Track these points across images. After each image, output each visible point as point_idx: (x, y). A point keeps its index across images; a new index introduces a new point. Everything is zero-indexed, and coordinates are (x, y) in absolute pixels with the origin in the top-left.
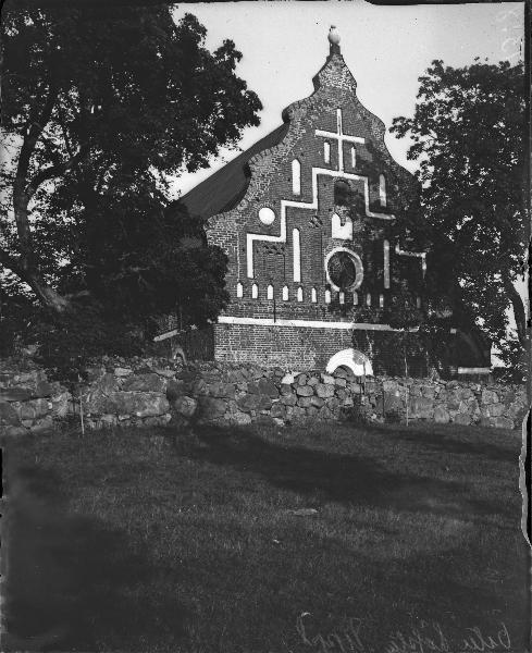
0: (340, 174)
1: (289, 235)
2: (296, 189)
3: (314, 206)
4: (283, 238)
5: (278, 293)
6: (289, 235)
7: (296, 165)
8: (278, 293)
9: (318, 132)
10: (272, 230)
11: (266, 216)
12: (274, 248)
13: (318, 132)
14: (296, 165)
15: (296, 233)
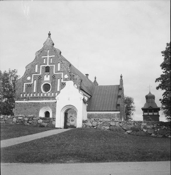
0: (48, 65)
1: (34, 82)
2: (36, 71)
3: (40, 74)
4: (32, 83)
5: (30, 95)
6: (34, 82)
7: (37, 66)
8: (30, 95)
9: (42, 57)
10: (30, 81)
11: (29, 78)
12: (29, 85)
13: (42, 57)
14: (37, 66)
15: (35, 81)
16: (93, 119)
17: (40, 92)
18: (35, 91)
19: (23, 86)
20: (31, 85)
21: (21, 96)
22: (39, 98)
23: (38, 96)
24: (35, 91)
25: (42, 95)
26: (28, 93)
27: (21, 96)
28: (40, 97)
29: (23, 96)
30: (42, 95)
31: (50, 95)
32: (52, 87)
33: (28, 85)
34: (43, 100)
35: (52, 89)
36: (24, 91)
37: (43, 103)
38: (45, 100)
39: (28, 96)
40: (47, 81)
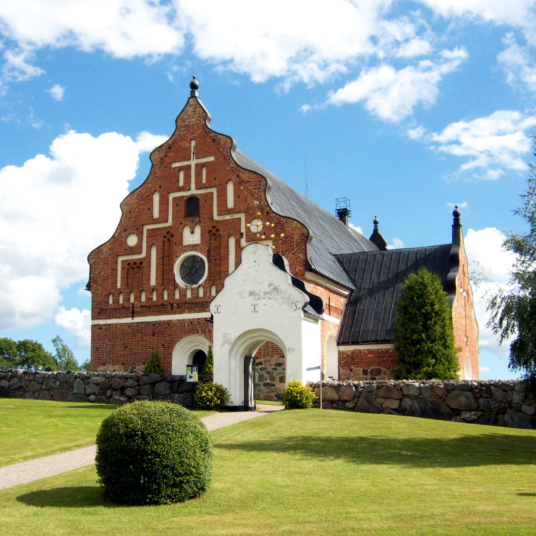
16: (361, 369)
17: (171, 287)
18: (153, 282)
19: (115, 270)
20: (141, 263)
21: (111, 301)
22: (169, 308)
23: (166, 298)
24: (153, 282)
25: (177, 296)
26: (131, 292)
27: (111, 301)
28: (172, 302)
29: (116, 301)
30: (177, 296)
31: (205, 293)
32: (209, 268)
33: (129, 264)
34: (182, 312)
35: (209, 272)
36: (119, 286)
37: (183, 321)
38: (190, 312)
39: (132, 300)
40: (193, 247)
